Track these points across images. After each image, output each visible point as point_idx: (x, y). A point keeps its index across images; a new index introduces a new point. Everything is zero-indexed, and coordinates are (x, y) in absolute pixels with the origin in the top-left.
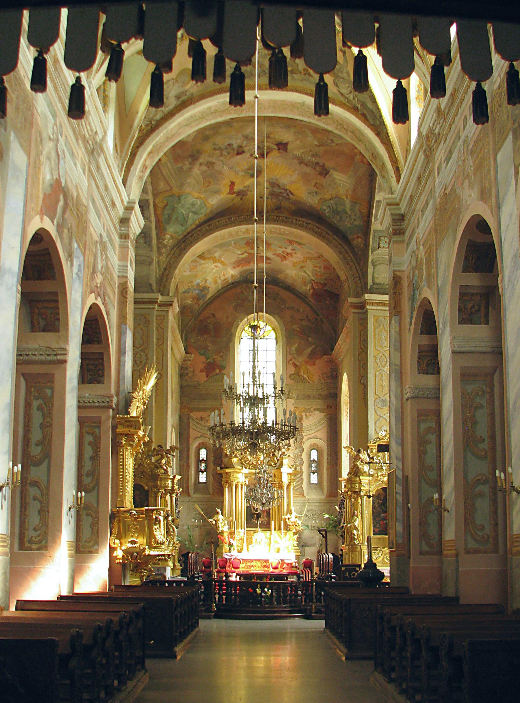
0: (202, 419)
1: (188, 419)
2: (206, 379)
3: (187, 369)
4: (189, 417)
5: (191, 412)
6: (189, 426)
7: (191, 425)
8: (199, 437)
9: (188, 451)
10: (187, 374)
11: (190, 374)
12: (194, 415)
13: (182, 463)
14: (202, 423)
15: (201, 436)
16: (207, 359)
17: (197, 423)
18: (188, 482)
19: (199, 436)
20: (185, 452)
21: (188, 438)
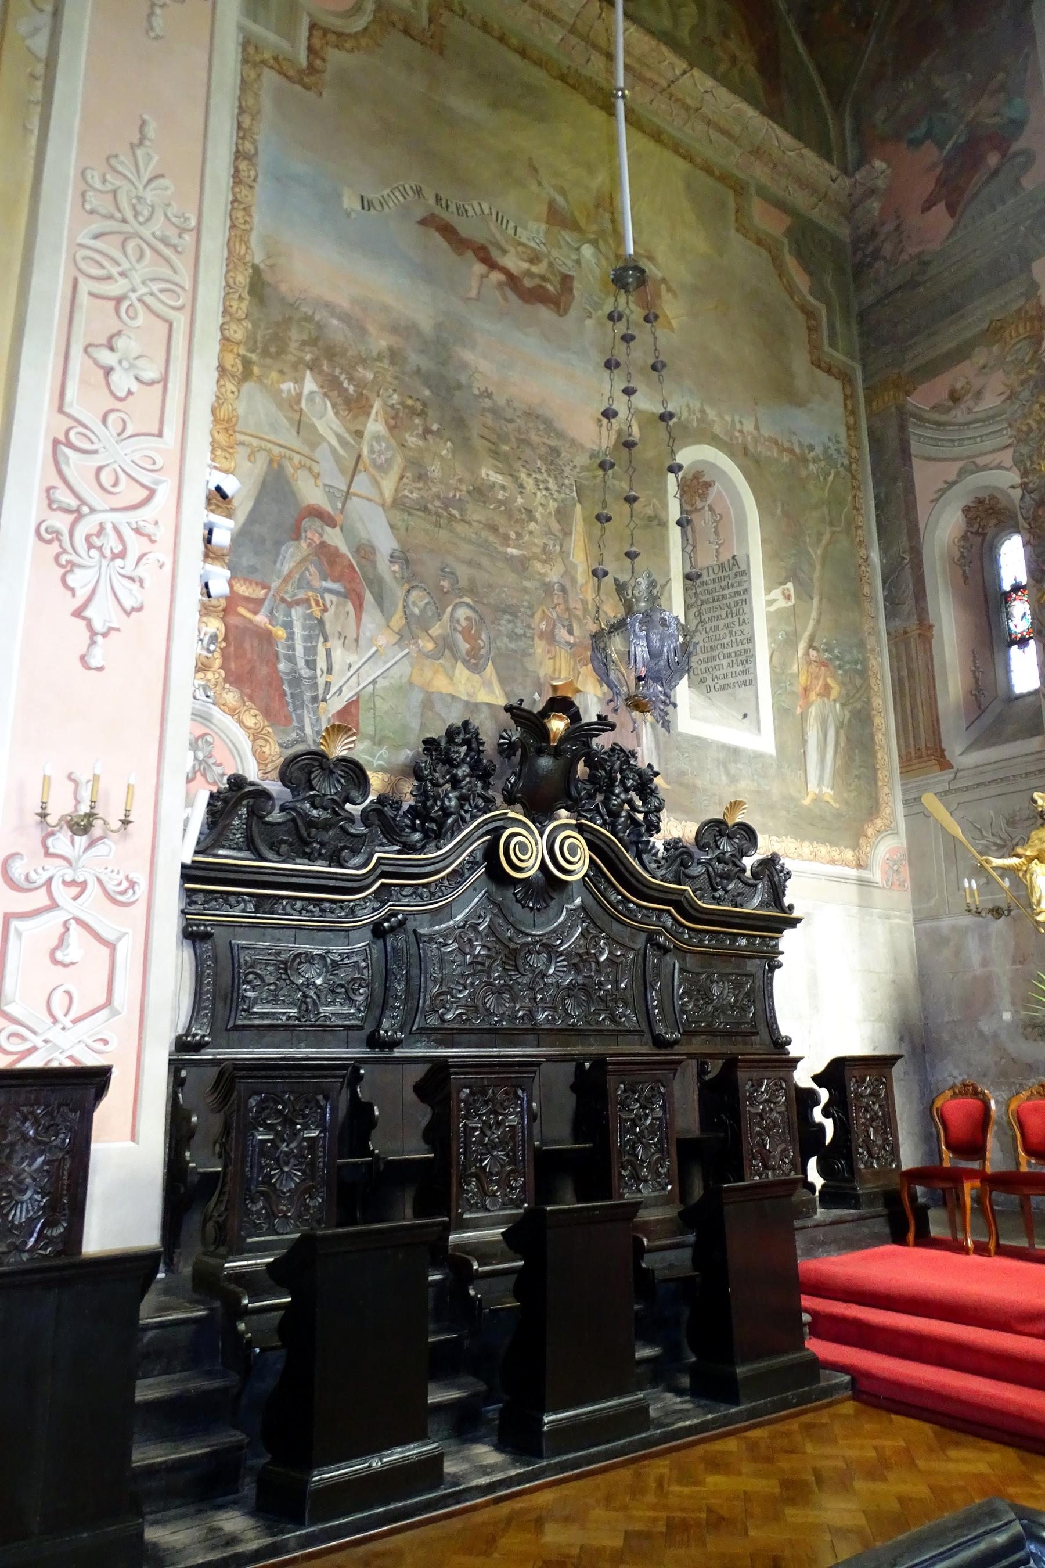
0: (955, 397)
1: (902, 428)
2: (950, 222)
3: (873, 234)
4: (903, 416)
5: (908, 393)
6: (905, 454)
7: (915, 447)
8: (951, 485)
9: (917, 565)
10: (876, 255)
11: (887, 249)
12: (921, 399)
13: (898, 623)
14: (959, 415)
15: (962, 473)
16: (941, 146)
17: (939, 424)
18: (932, 701)
19: (952, 477)
20: (908, 571)
21: (911, 506)
